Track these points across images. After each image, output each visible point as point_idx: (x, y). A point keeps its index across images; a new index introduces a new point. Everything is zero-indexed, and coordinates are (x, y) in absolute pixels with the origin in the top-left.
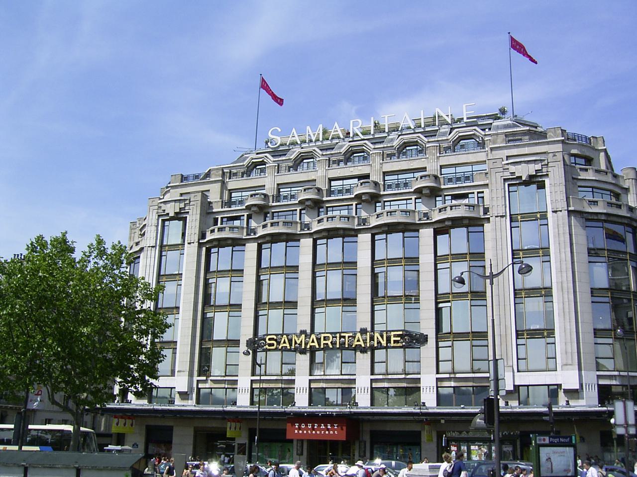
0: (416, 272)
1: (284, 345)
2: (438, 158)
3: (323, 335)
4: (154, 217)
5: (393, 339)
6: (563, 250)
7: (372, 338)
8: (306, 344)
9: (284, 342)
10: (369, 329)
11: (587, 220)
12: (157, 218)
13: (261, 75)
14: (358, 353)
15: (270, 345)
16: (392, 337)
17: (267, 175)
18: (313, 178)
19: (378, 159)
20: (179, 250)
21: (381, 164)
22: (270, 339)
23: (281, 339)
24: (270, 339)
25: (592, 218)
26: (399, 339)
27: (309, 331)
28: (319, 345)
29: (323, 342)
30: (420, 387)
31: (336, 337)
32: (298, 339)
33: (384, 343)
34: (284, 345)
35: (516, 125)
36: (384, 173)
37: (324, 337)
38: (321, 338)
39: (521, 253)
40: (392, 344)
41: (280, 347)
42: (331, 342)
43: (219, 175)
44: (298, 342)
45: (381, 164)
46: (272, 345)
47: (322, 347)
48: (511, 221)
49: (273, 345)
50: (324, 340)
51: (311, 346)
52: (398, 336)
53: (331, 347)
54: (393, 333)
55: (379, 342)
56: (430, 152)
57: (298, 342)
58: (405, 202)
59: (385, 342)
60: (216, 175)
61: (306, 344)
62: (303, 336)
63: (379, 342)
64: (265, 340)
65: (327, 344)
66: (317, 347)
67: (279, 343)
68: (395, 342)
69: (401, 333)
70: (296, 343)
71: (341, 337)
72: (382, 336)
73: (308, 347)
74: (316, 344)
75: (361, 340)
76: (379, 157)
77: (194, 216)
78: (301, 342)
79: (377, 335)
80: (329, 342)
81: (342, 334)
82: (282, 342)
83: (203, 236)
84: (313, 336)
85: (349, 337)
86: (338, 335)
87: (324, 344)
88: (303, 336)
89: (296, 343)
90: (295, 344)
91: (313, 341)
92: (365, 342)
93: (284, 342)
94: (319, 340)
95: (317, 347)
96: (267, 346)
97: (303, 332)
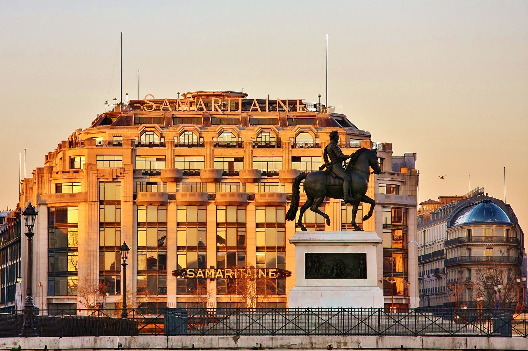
0: (284, 232)
1: (200, 275)
2: (291, 151)
3: (226, 270)
4: (94, 179)
5: (270, 274)
6: (370, 226)
7: (258, 273)
8: (215, 275)
9: (200, 274)
10: (255, 266)
11: (384, 207)
12: (97, 180)
13: (121, 33)
14: (248, 280)
16: (270, 272)
17: (167, 148)
18: (203, 154)
19: (250, 147)
20: (115, 205)
21: (252, 150)
22: (190, 271)
23: (198, 271)
24: (190, 271)
25: (386, 206)
26: (274, 274)
27: (215, 267)
28: (224, 275)
29: (226, 274)
30: (286, 303)
31: (234, 271)
32: (210, 272)
33: (265, 276)
34: (200, 275)
35: (339, 125)
36: (254, 157)
37: (227, 271)
38: (224, 271)
39: (346, 226)
40: (270, 277)
42: (231, 275)
43: (129, 144)
44: (210, 273)
45: (252, 150)
46: (192, 275)
47: (225, 277)
48: (342, 206)
49: (192, 275)
50: (227, 273)
51: (218, 276)
52: (274, 272)
53: (231, 277)
54: (270, 270)
55: (262, 275)
56: (286, 146)
57: (210, 273)
58: (274, 184)
59: (266, 275)
60: (126, 144)
61: (215, 275)
62: (213, 271)
63: (262, 275)
64: (186, 272)
65: (228, 276)
66: (222, 277)
67: (196, 274)
68: (272, 275)
69: (275, 270)
70: (208, 274)
71: (238, 271)
72: (264, 272)
73: (216, 277)
74: (221, 275)
75: (250, 273)
76: (250, 145)
77: (128, 182)
78: (212, 273)
79: (260, 271)
81: (238, 270)
82: (198, 273)
83: (135, 197)
84: (219, 270)
85: (243, 271)
86: (236, 270)
87: (227, 275)
88: (212, 271)
89: (208, 274)
90: (208, 275)
91: (219, 274)
92: (253, 274)
94: (223, 273)
95: (222, 277)
96: (188, 276)
97: (212, 267)
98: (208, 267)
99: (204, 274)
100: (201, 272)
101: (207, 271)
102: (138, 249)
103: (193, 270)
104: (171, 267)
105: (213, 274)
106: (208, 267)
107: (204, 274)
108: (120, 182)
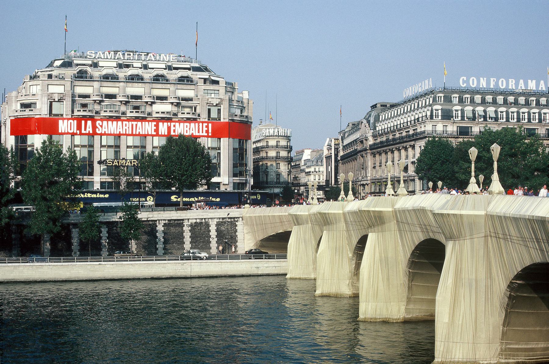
1: (116, 164)
8: (126, 164)
9: (116, 163)
15: (109, 164)
22: (109, 161)
24: (109, 161)
29: (133, 163)
41: (114, 165)
46: (110, 164)
49: (110, 164)
57: (122, 163)
61: (126, 164)
64: (106, 161)
67: (113, 163)
70: (121, 163)
80: (135, 164)
89: (121, 163)
93: (116, 163)
97: (123, 159)
98: (121, 158)
99: (118, 162)
100: (117, 162)
101: (120, 161)
102: (74, 146)
103: (111, 160)
104: (96, 159)
105: (124, 163)
106: (121, 158)
107: (118, 162)
108: (63, 102)
